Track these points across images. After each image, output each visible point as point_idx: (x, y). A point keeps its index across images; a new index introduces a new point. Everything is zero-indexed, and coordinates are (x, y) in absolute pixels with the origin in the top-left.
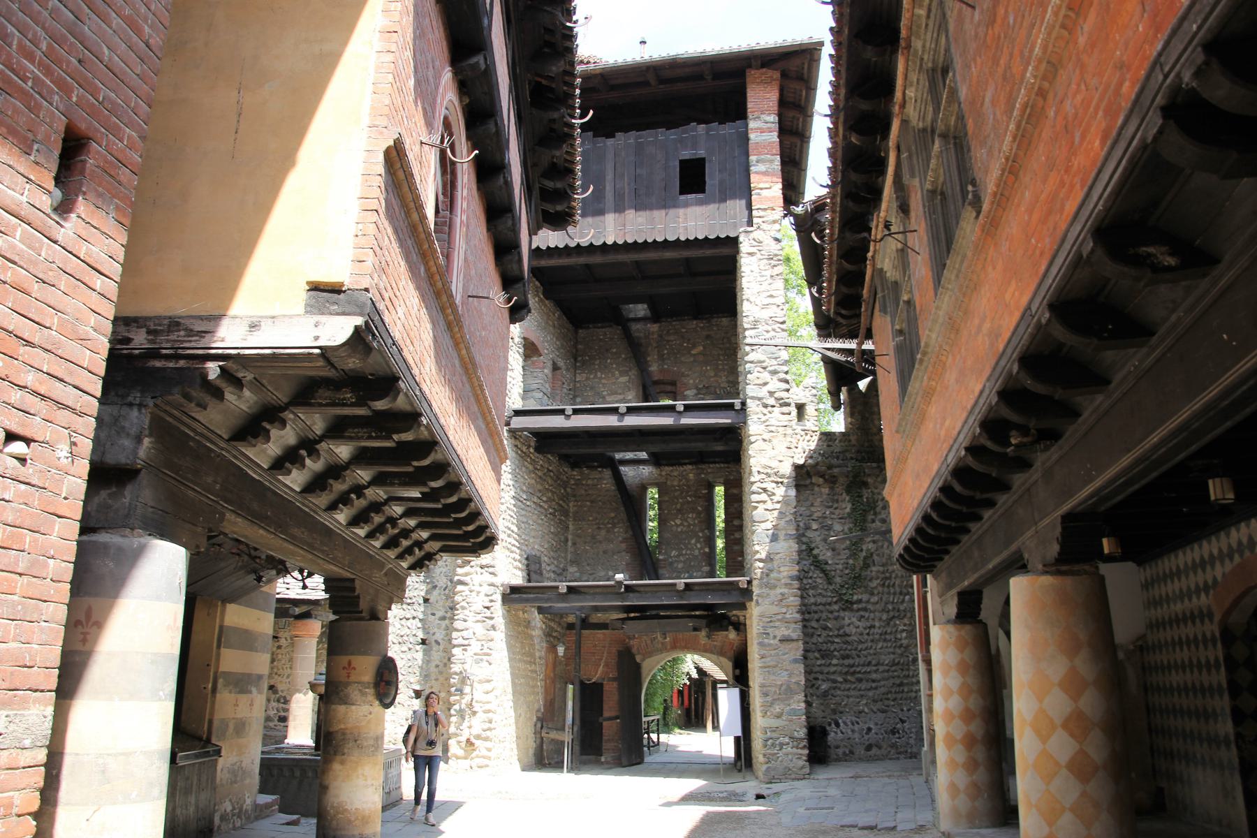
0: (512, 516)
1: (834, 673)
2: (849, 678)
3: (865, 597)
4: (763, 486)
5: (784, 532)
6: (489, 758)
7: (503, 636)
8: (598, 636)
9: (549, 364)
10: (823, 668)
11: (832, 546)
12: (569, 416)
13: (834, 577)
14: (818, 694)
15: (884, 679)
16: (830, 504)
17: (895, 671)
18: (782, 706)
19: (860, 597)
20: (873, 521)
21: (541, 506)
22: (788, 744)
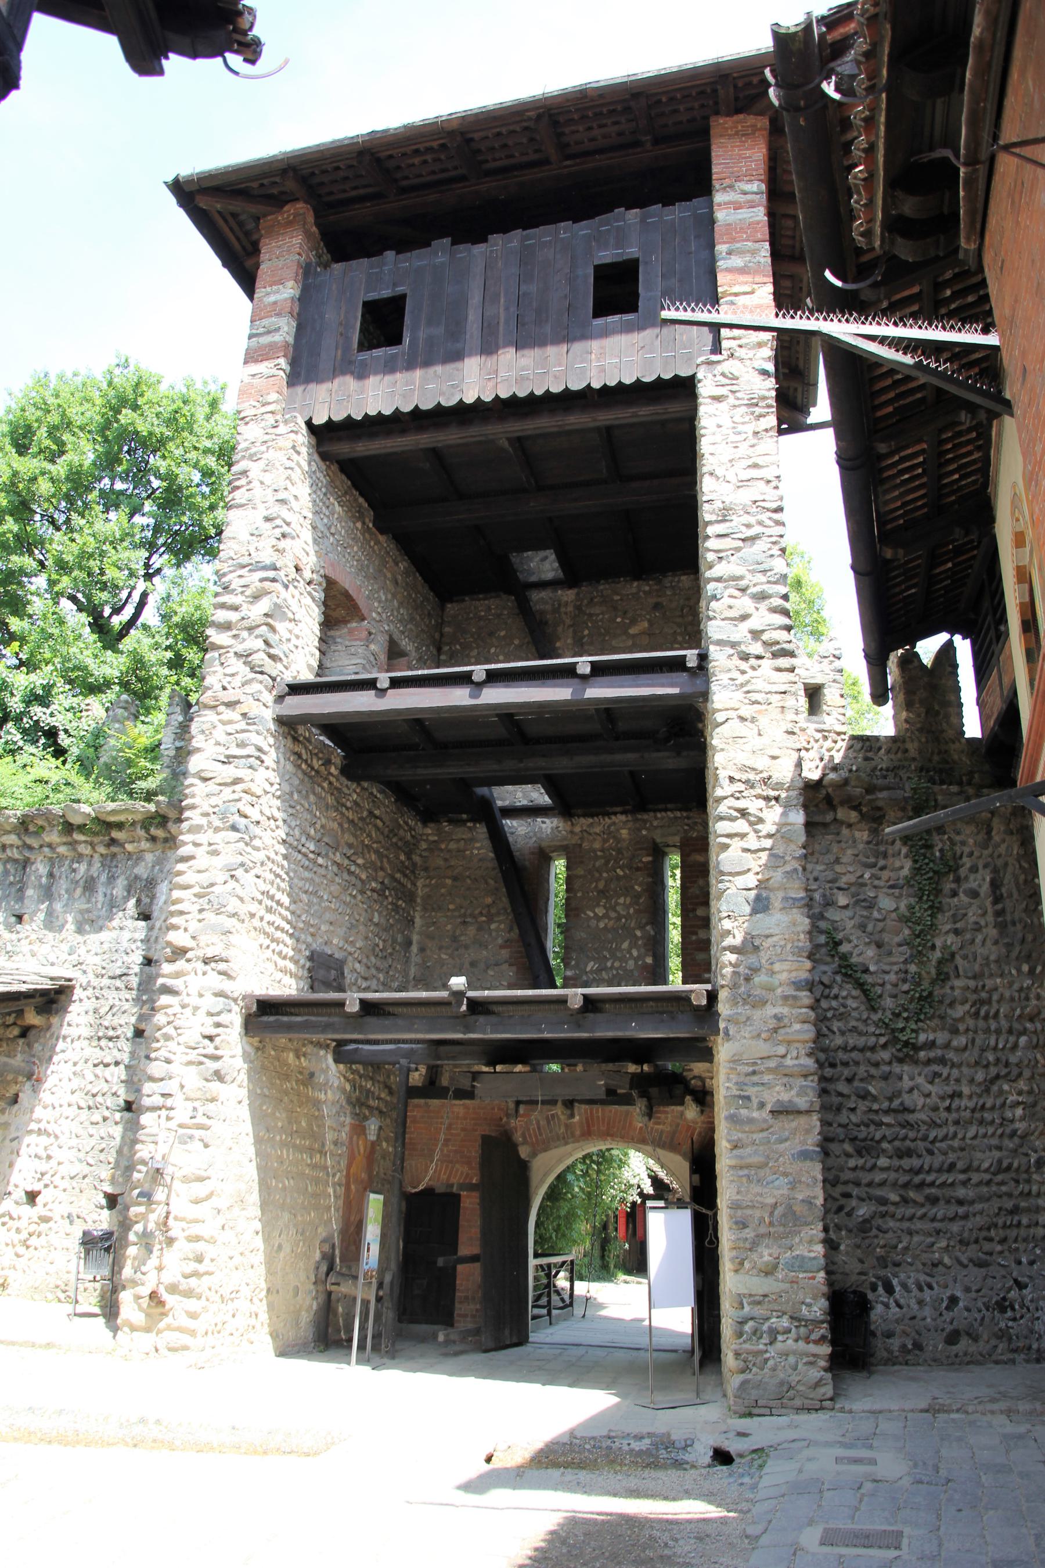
0: (278, 876)
1: (883, 1184)
2: (912, 1194)
3: (941, 1037)
4: (741, 804)
5: (780, 894)
6: (193, 1333)
7: (243, 1093)
8: (456, 1109)
9: (382, 639)
10: (860, 1174)
11: (876, 937)
12: (385, 690)
13: (880, 996)
14: (851, 1225)
15: (982, 1199)
16: (872, 860)
17: (1002, 1183)
18: (775, 1251)
19: (931, 1037)
20: (954, 894)
21: (350, 873)
22: (788, 1331)
